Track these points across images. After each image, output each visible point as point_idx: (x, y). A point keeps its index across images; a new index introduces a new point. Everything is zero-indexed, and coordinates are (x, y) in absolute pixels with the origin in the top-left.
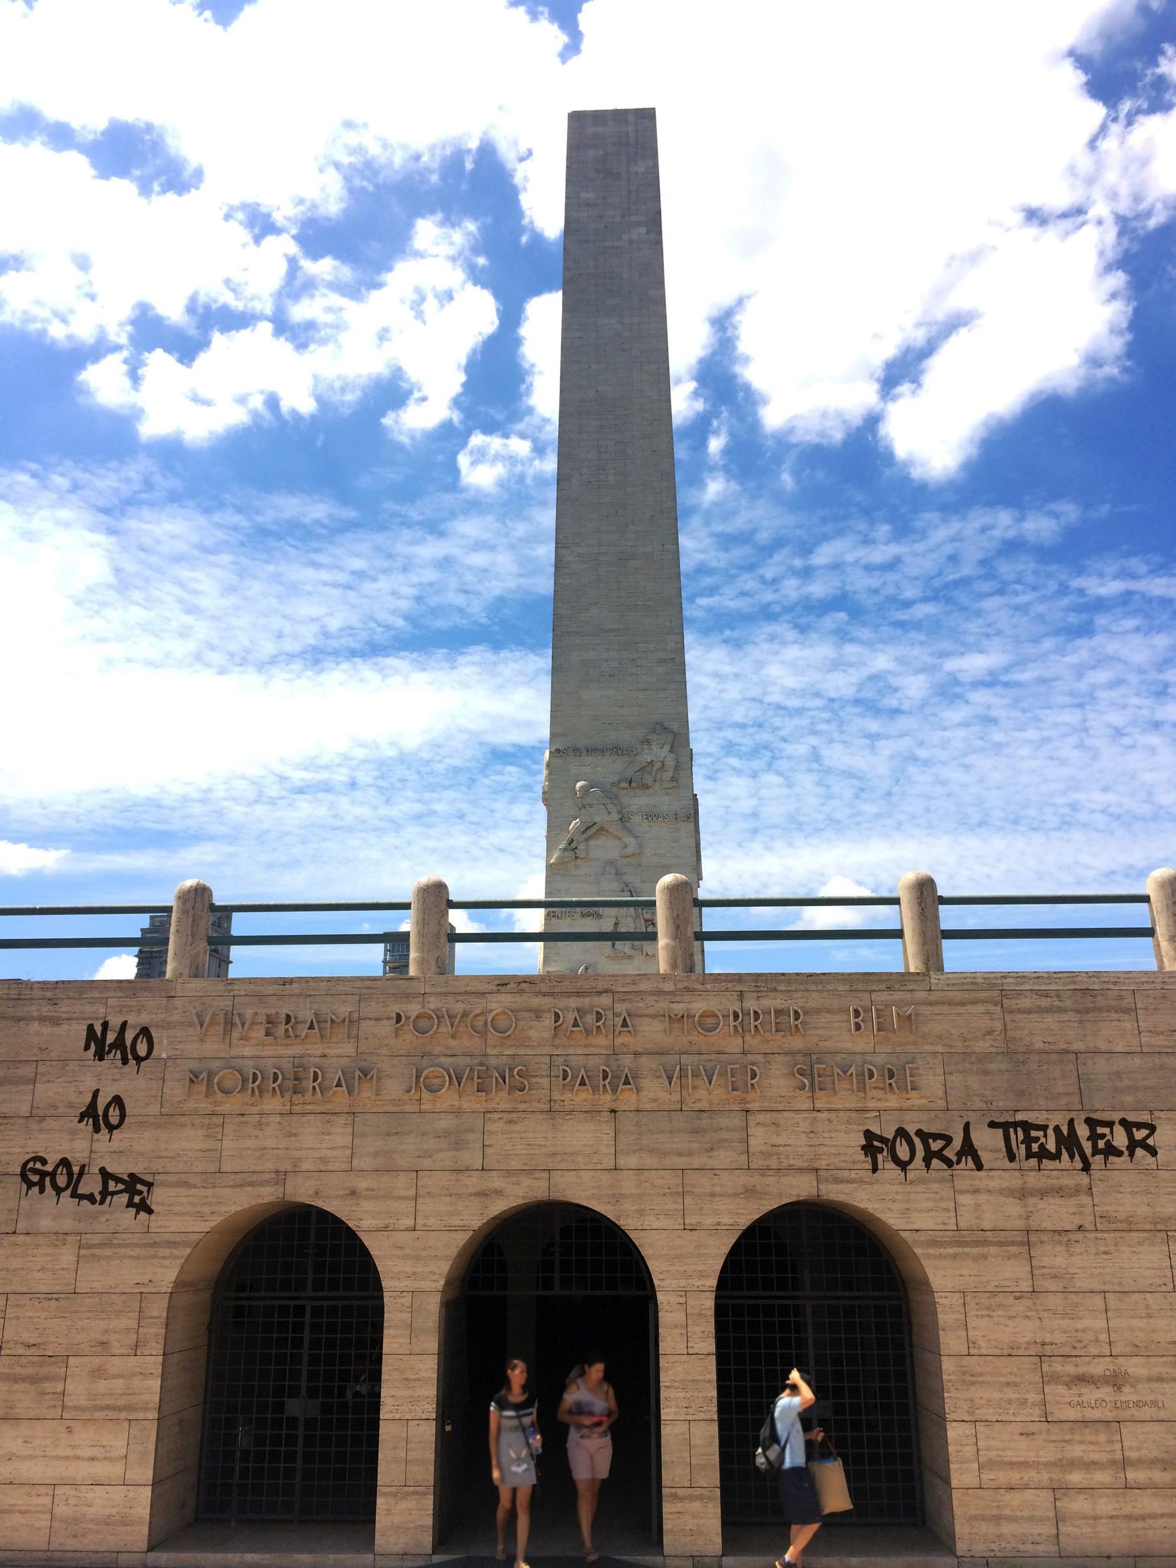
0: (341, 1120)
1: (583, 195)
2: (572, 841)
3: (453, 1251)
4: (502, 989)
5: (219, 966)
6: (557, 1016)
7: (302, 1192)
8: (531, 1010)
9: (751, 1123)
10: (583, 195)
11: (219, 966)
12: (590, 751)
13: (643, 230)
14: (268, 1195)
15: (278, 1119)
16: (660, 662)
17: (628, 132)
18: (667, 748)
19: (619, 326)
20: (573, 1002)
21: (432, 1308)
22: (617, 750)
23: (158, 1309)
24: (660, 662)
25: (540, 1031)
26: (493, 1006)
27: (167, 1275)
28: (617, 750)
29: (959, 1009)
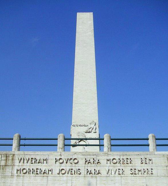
0: (45, 177)
4: (76, 154)
6: (86, 159)
8: (81, 158)
9: (122, 179)
12: (80, 126)
13: (90, 33)
15: (33, 177)
20: (89, 157)
22: (85, 126)
26: (74, 157)
28: (85, 126)
29: (160, 158)
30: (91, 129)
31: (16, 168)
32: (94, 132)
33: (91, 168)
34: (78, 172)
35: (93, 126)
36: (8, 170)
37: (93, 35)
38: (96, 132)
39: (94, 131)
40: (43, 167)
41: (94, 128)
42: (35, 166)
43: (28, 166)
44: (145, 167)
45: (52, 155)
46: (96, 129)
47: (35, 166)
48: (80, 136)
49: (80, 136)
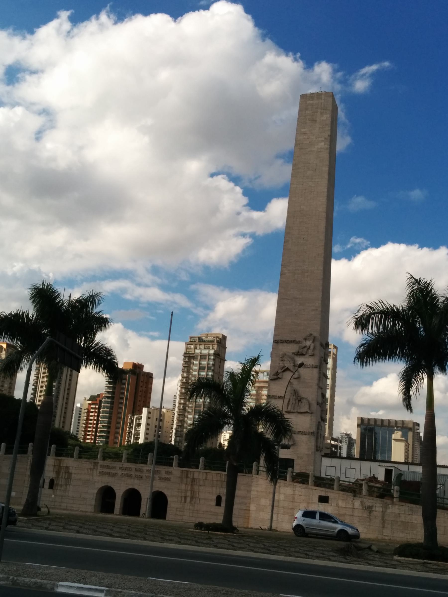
1: (303, 130)
2: (277, 372)
3: (123, 492)
5: (220, 362)
7: (109, 485)
10: (303, 130)
11: (220, 362)
13: (323, 144)
14: (106, 485)
16: (313, 310)
17: (321, 103)
18: (311, 341)
19: (311, 183)
21: (120, 497)
22: (294, 342)
23: (95, 495)
24: (313, 310)
25: (134, 470)
27: (96, 491)
28: (294, 342)
30: (305, 349)
31: (98, 470)
32: (310, 354)
33: (138, 474)
34: (129, 476)
35: (308, 343)
36: (95, 471)
37: (327, 149)
38: (313, 355)
39: (310, 352)
40: (113, 471)
41: (312, 347)
42: (108, 471)
43: (105, 470)
44: (166, 476)
45: (118, 465)
46: (314, 348)
47: (108, 471)
48: (284, 360)
49: (284, 360)
